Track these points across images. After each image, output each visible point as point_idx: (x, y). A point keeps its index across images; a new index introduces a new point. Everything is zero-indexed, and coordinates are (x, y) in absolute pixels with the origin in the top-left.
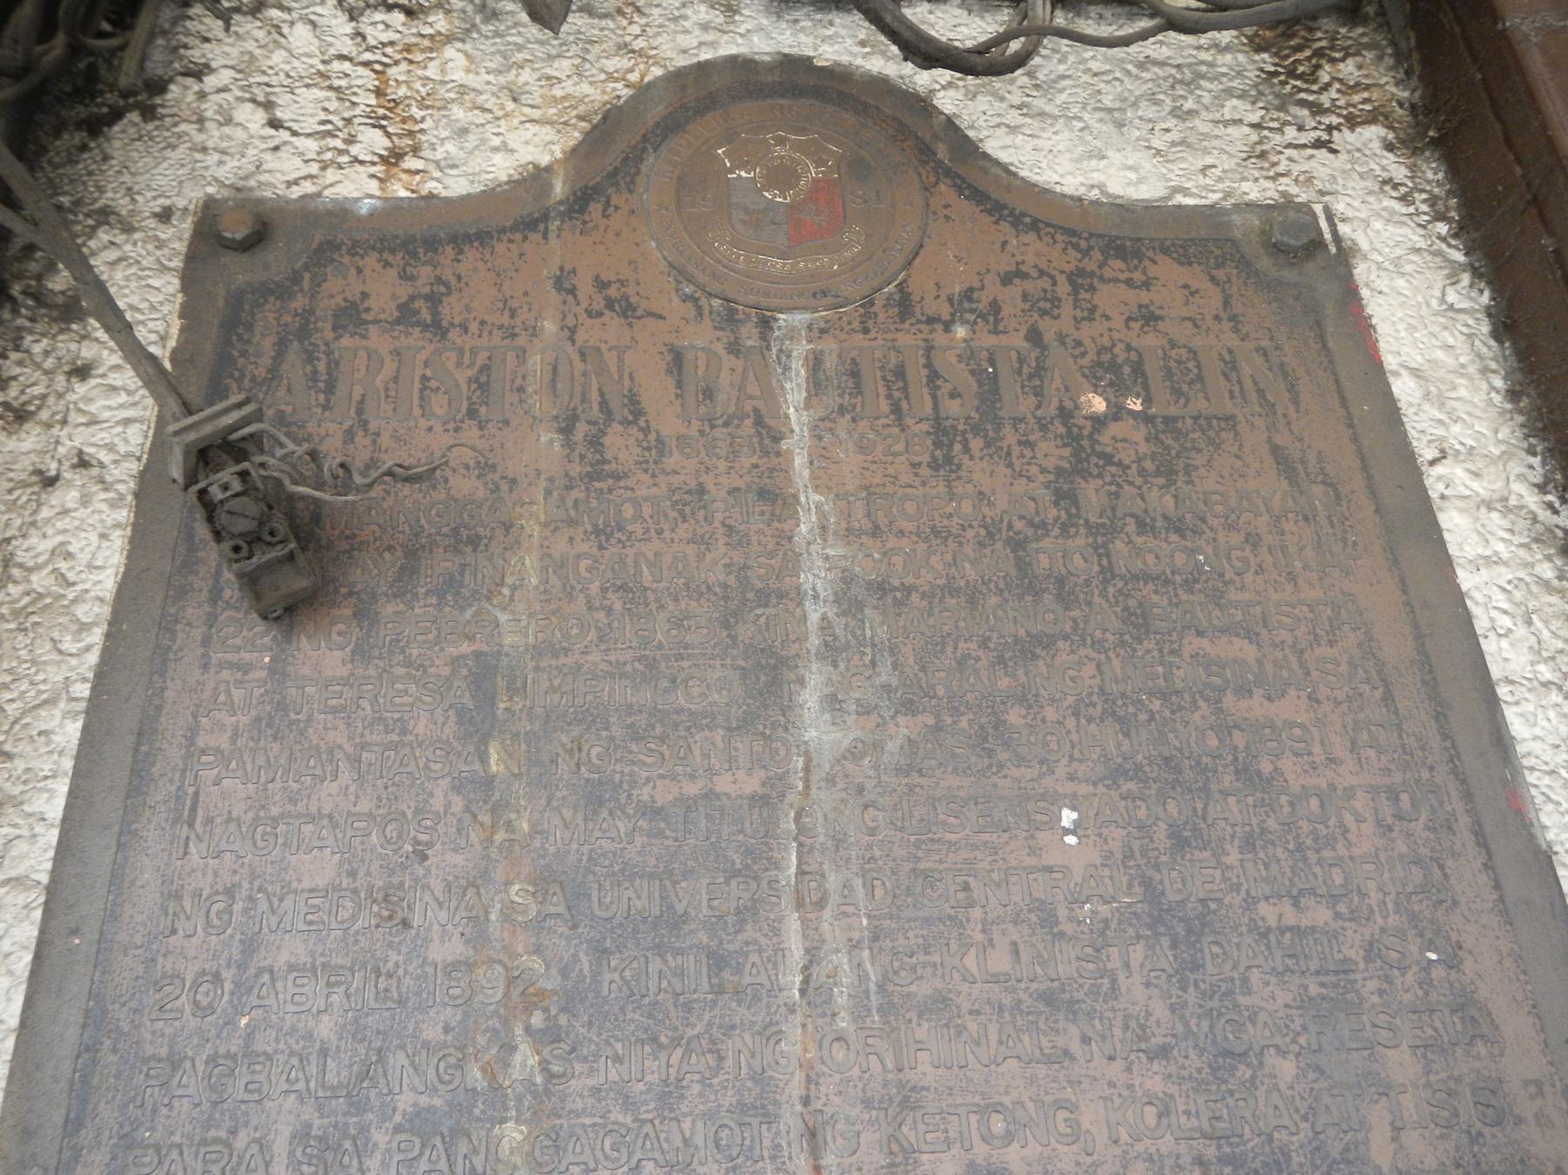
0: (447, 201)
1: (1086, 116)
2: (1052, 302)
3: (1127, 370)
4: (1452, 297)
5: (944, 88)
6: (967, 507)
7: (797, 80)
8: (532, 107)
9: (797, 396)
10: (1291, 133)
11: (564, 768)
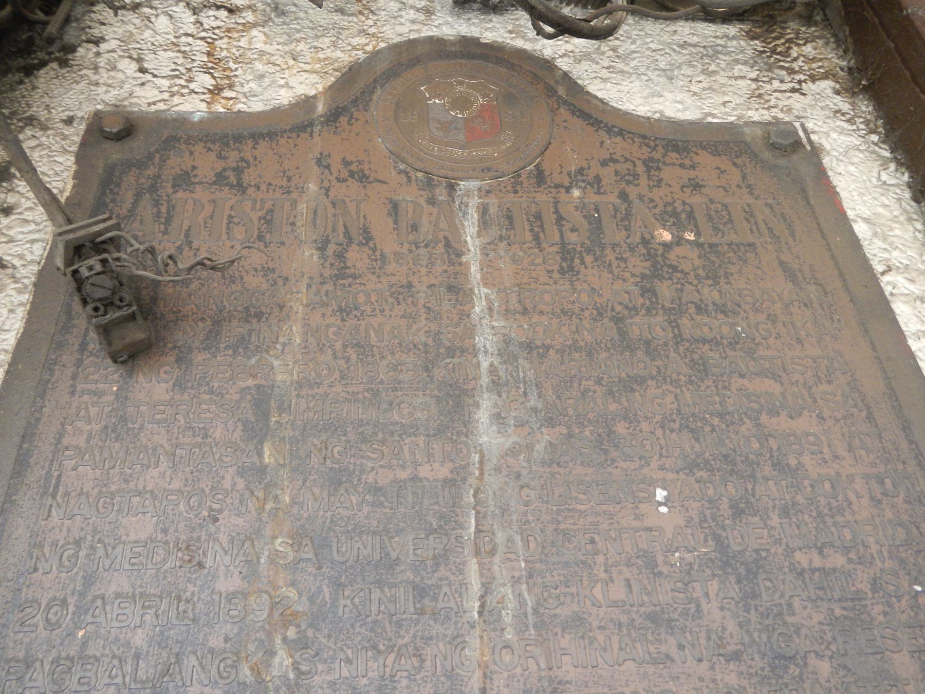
0: (250, 114)
2: (633, 176)
3: (684, 216)
4: (884, 177)
5: (561, 57)
6: (584, 298)
7: (470, 50)
8: (305, 63)
9: (472, 230)
10: (776, 84)
11: (315, 460)
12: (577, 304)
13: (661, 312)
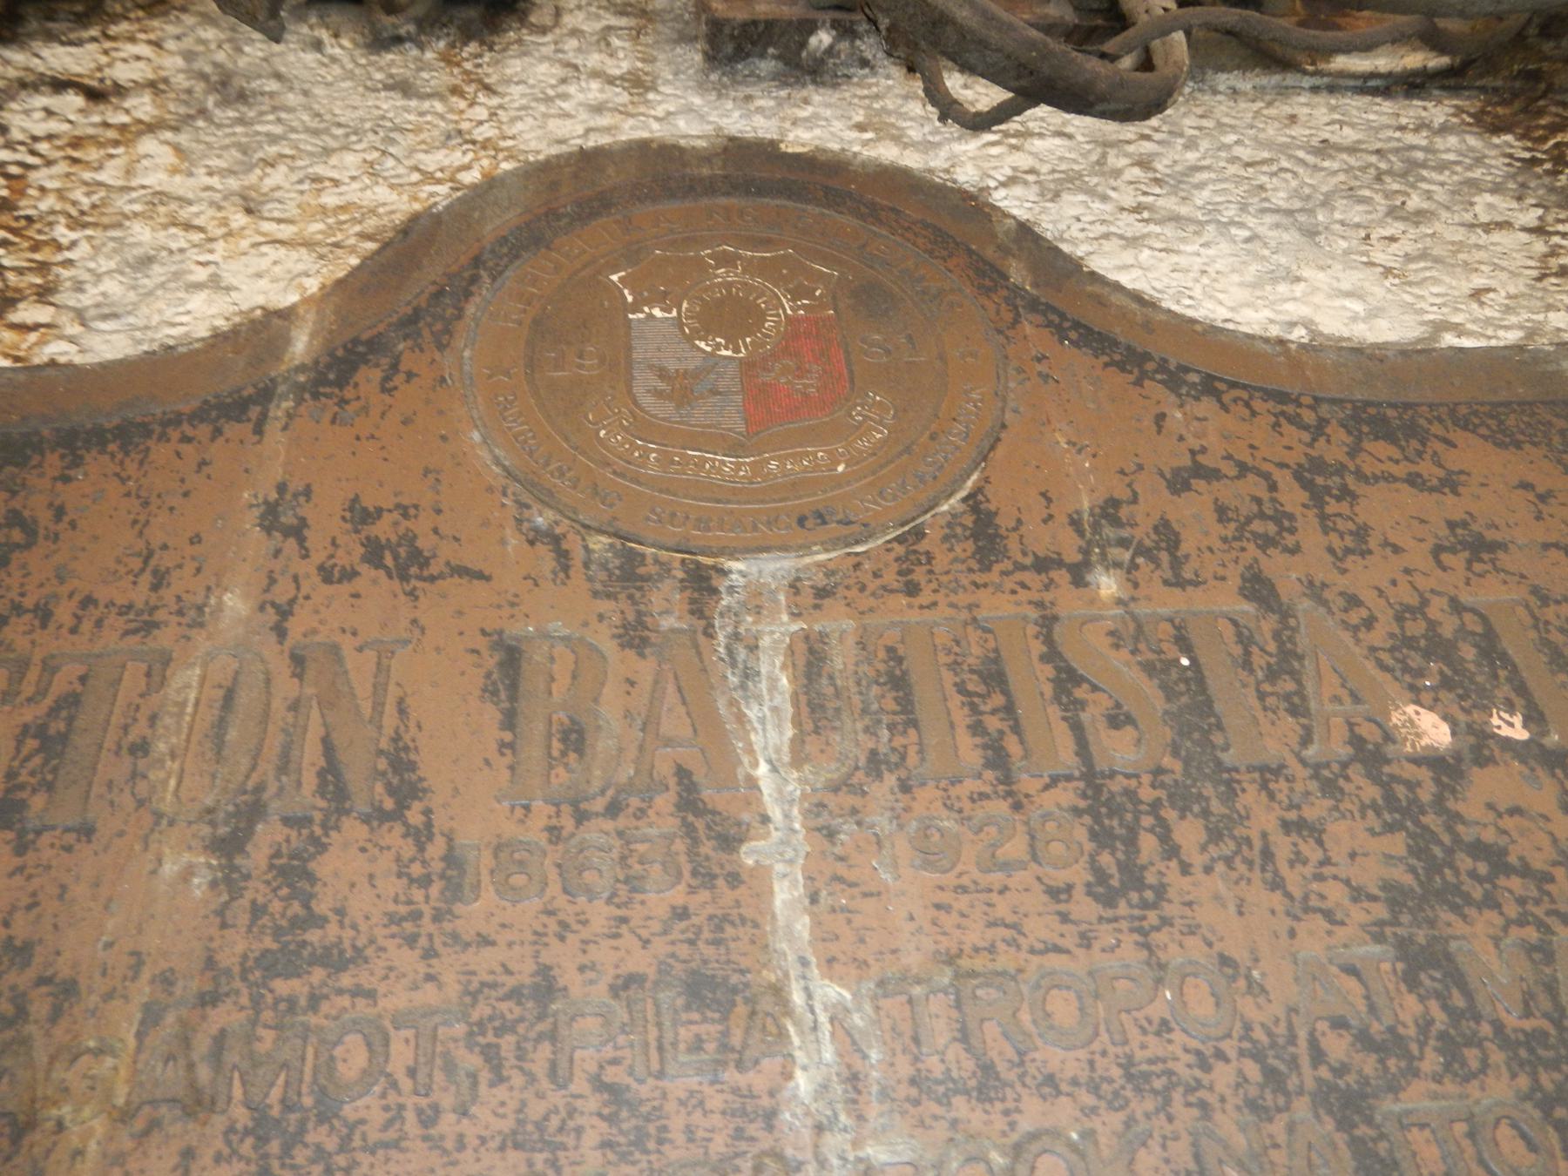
1: (1251, 221)
2: (1278, 522)
3: (1468, 652)
9: (772, 734)
12: (1177, 1036)
13: (1498, 1057)
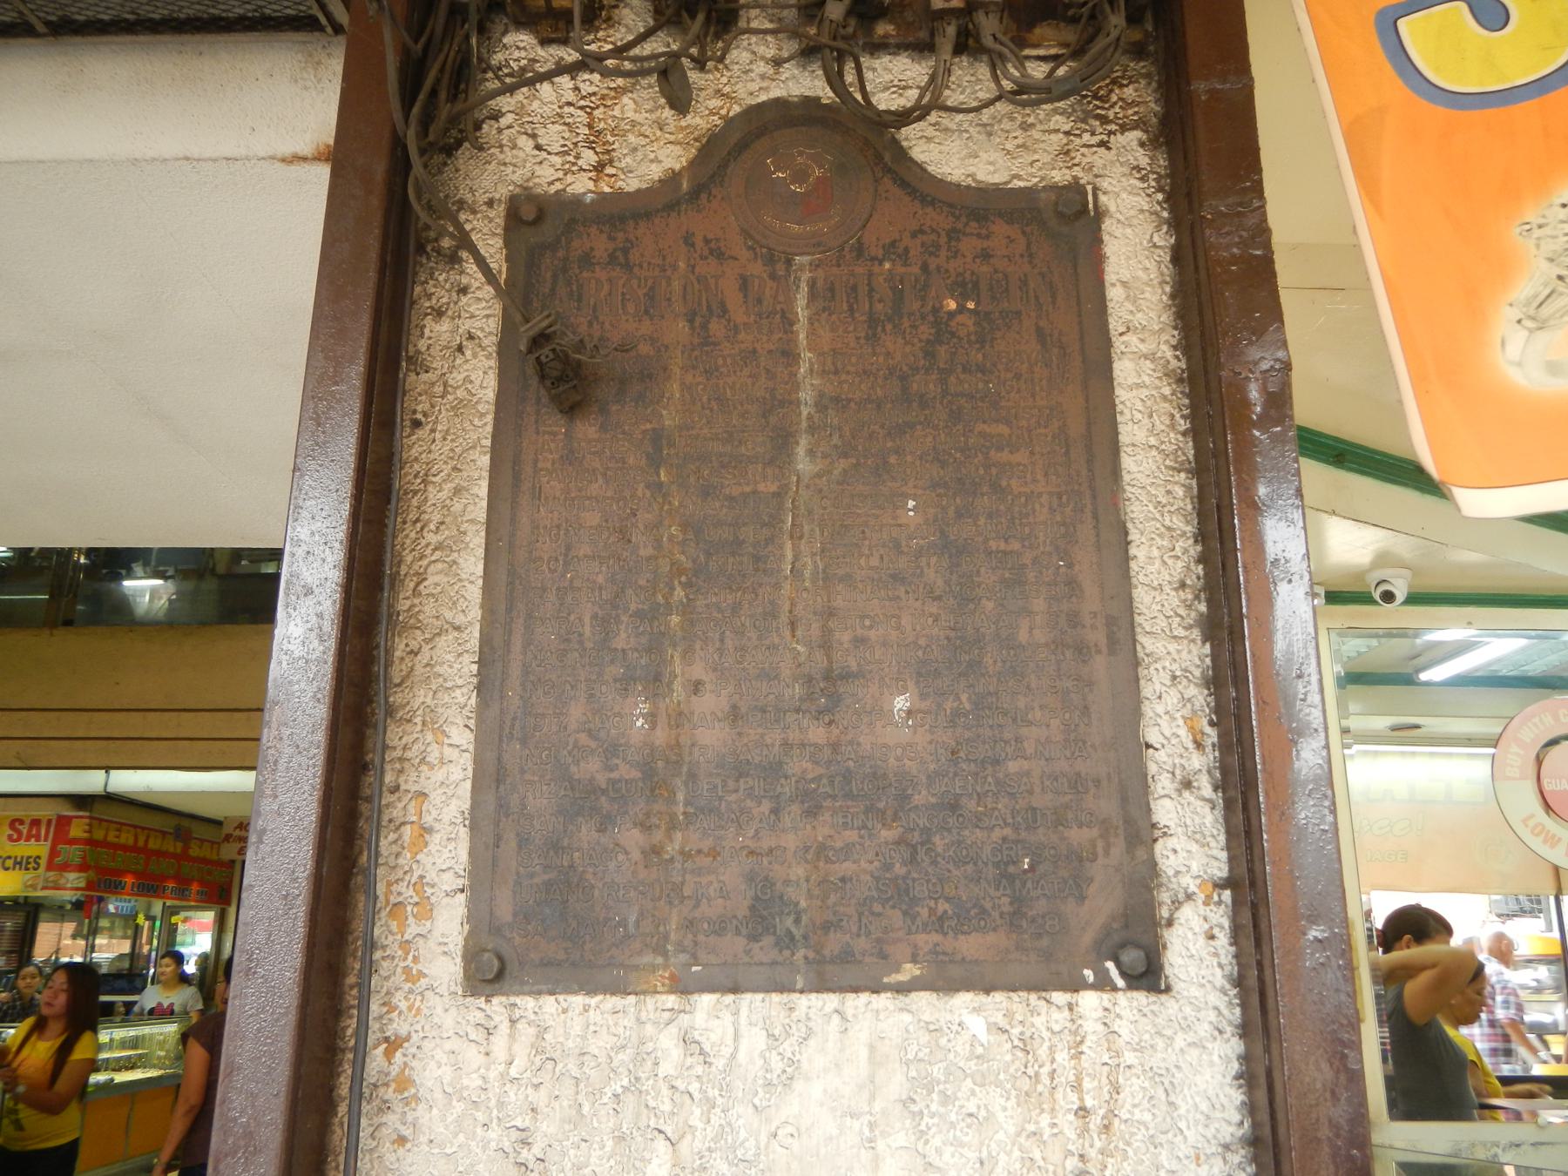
6: (881, 359)
